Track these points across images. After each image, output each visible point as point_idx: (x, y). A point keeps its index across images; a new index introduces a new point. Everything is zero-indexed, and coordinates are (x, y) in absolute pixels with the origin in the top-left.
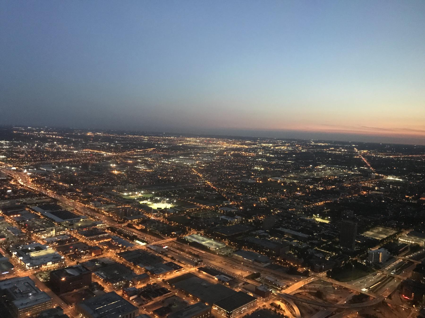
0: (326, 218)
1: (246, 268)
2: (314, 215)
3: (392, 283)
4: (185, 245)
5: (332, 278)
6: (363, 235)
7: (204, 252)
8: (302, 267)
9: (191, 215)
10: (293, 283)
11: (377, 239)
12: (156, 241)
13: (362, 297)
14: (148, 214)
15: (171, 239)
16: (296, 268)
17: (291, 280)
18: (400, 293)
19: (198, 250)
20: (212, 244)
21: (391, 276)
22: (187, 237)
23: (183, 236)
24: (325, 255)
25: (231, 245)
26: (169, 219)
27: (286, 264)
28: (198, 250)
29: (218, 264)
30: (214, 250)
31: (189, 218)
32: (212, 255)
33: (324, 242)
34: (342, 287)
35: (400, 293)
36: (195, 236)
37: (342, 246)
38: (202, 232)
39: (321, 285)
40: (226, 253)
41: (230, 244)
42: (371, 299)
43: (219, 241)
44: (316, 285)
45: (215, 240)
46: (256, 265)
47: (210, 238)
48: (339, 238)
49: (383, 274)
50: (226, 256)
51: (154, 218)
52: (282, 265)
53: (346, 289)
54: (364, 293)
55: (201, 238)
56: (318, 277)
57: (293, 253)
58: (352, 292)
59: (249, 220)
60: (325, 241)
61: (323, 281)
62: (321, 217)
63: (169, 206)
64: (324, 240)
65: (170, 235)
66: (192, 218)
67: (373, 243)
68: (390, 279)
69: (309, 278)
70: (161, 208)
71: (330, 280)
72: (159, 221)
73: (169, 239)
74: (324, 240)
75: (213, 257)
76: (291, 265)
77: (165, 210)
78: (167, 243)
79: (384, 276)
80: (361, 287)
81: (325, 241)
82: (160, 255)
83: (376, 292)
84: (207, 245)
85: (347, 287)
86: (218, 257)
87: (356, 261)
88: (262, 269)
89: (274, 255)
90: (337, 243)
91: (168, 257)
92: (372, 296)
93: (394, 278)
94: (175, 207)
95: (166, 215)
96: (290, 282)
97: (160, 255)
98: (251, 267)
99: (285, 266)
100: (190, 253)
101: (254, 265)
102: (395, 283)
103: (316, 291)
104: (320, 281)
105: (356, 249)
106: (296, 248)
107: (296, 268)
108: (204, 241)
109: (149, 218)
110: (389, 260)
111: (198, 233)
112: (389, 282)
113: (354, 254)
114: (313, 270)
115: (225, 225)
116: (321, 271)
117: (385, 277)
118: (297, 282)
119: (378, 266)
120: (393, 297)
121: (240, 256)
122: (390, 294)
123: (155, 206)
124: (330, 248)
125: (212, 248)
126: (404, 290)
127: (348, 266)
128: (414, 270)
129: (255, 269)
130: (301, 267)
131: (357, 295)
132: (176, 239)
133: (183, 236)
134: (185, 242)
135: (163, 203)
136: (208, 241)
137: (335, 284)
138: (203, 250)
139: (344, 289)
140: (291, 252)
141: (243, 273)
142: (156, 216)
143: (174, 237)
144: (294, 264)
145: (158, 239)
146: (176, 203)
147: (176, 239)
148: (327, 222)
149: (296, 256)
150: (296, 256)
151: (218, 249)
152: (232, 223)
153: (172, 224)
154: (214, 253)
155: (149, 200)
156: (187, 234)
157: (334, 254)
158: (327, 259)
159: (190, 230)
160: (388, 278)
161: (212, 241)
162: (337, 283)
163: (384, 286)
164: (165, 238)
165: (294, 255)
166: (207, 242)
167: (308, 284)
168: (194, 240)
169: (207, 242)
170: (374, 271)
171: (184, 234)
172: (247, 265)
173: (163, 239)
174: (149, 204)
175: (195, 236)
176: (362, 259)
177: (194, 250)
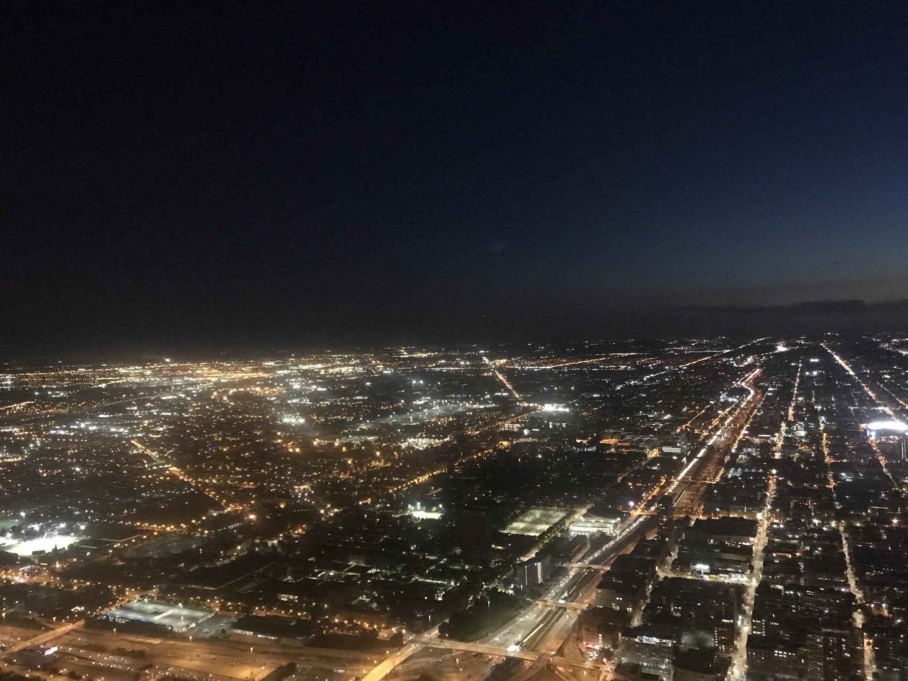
0: (434, 509)
1: (262, 658)
2: (410, 506)
3: (562, 622)
4: (107, 634)
5: (451, 637)
6: (505, 532)
7: (157, 641)
10: (370, 668)
11: (532, 534)
12: (25, 639)
13: (512, 663)
14: (7, 570)
15: (70, 627)
16: (374, 633)
17: (366, 663)
18: (579, 639)
19: (143, 640)
20: (177, 617)
21: (560, 608)
22: (115, 612)
23: (103, 612)
25: (227, 610)
26: (66, 575)
27: (355, 627)
28: (143, 640)
30: (184, 630)
32: (180, 643)
34: (471, 652)
35: (578, 640)
36: (139, 606)
37: (468, 564)
38: (154, 592)
40: (213, 632)
41: (223, 607)
42: (527, 664)
43: (196, 606)
45: (186, 605)
46: (283, 646)
47: (174, 604)
49: (546, 606)
50: (212, 640)
51: (22, 581)
52: (345, 632)
53: (479, 655)
54: (512, 655)
55: (151, 607)
56: (422, 643)
57: (368, 600)
58: (490, 660)
59: (270, 543)
60: (435, 558)
64: (431, 558)
65: (64, 614)
67: (523, 543)
68: (561, 611)
69: (403, 649)
70: (43, 552)
71: (447, 644)
72: (36, 587)
73: (62, 626)
74: (431, 558)
75: (184, 649)
76: (365, 629)
77: (57, 554)
79: (549, 609)
80: (504, 644)
81: (435, 558)
82: (37, 674)
83: (536, 646)
84: (167, 622)
85: (480, 651)
86: (196, 644)
87: (496, 589)
88: (299, 651)
89: (326, 612)
90: (454, 559)
91: (61, 674)
92: (529, 658)
93: (565, 609)
94: (82, 542)
95: (58, 566)
96: (361, 667)
97: (37, 674)
98: (274, 653)
99: (351, 633)
100: (120, 652)
101: (283, 646)
102: (569, 619)
103: (418, 677)
104: (427, 651)
105: (496, 562)
106: (376, 585)
107: (374, 633)
108: (157, 613)
109: (9, 581)
110: (555, 574)
111: (143, 597)
112: (558, 620)
113: (491, 575)
114: (412, 629)
115: (213, 563)
116: (427, 627)
117: (550, 612)
118: (378, 664)
119: (537, 592)
120: (566, 651)
121: (248, 633)
122: (559, 646)
123: (24, 548)
124: (445, 573)
125: (180, 626)
126: (584, 632)
128: (599, 587)
129: (284, 655)
130: (386, 628)
131: (500, 662)
132: (82, 623)
133: (103, 612)
134: (108, 624)
135: (50, 536)
136: (171, 611)
138: (154, 636)
139: (475, 656)
141: (256, 670)
142: (30, 573)
143: (78, 619)
144: (371, 625)
145: (30, 632)
146: (85, 532)
147: (82, 623)
148: (436, 516)
150: (375, 605)
151: (194, 625)
153: (72, 587)
154: (182, 637)
155: (9, 535)
156: (114, 604)
157: (453, 583)
158: (440, 599)
159: (121, 592)
160: (556, 613)
161: (180, 610)
162: (462, 646)
163: (549, 630)
164: (51, 626)
165: (371, 602)
166: (160, 616)
167: (401, 663)
168: (132, 616)
169: (164, 615)
170: (529, 604)
172: (263, 651)
173: (48, 629)
174: (10, 547)
175: (135, 604)
176: (507, 584)
177: (131, 641)
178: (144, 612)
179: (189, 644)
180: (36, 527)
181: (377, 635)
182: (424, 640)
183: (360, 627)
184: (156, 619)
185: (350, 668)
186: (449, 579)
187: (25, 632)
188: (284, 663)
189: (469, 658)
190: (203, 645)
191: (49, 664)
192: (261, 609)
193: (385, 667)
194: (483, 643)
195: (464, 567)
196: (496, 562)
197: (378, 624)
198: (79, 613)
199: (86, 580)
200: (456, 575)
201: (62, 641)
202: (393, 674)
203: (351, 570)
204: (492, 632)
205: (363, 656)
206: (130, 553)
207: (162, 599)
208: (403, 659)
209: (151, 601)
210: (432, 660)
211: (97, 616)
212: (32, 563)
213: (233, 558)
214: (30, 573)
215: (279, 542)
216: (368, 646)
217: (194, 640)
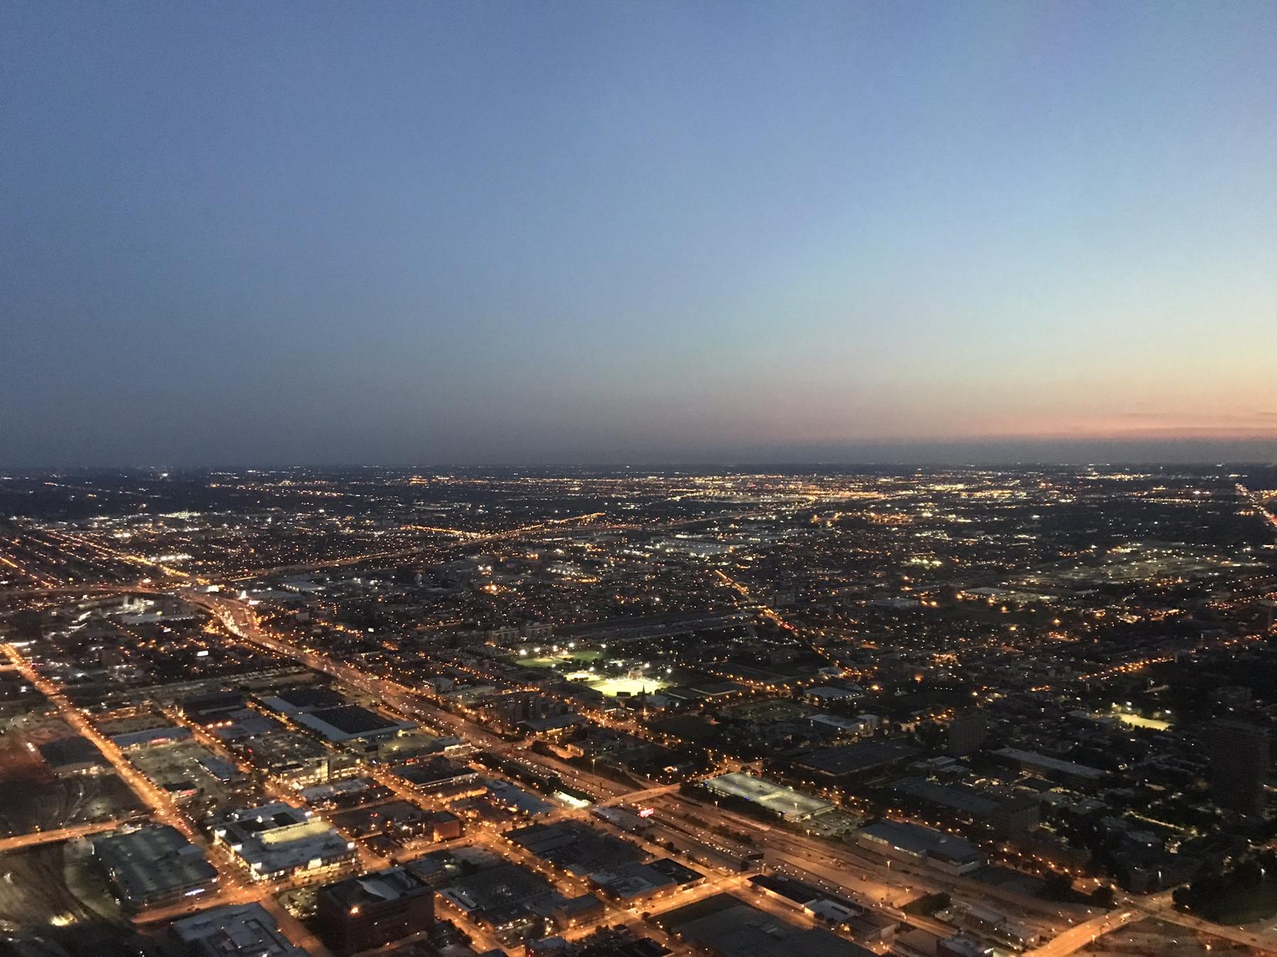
0: (1157, 715)
1: (900, 877)
2: (1114, 705)
4: (706, 807)
5: (1192, 912)
7: (766, 828)
8: (1089, 875)
9: (722, 714)
10: (1061, 928)
12: (618, 794)
14: (592, 710)
15: (664, 789)
16: (1066, 881)
17: (1054, 919)
22: (712, 781)
24: (1165, 835)
25: (851, 804)
26: (654, 726)
27: (1035, 865)
29: (811, 866)
31: (713, 722)
32: (793, 836)
33: (1159, 795)
34: (1230, 941)
36: (735, 779)
37: (1221, 808)
38: (757, 765)
39: (1156, 936)
40: (834, 831)
41: (845, 801)
43: (812, 792)
44: (1139, 935)
45: (798, 788)
47: (784, 785)
48: (1207, 780)
50: (834, 841)
52: (1019, 869)
53: (1243, 948)
55: (754, 784)
56: (1147, 911)
59: (904, 727)
60: (1161, 788)
61: (1164, 922)
62: (1140, 712)
63: (652, 686)
64: (1155, 787)
66: (724, 721)
69: (1114, 913)
70: (628, 694)
71: (1187, 921)
72: (623, 733)
74: (1155, 787)
76: (1050, 870)
78: (652, 800)
81: (1161, 788)
82: (631, 838)
84: (775, 806)
86: (811, 842)
88: (950, 880)
89: (989, 834)
90: (1201, 797)
91: (658, 844)
94: (670, 689)
95: (645, 713)
96: (1048, 925)
97: (631, 838)
98: (917, 875)
99: (1029, 872)
100: (722, 831)
101: (928, 868)
104: (1151, 922)
106: (1063, 812)
107: (1066, 881)
108: (763, 793)
109: (595, 723)
111: (744, 769)
114: (1126, 885)
115: (828, 742)
116: (1154, 888)
118: (1077, 923)
121: (881, 841)
123: (610, 687)
124: (1182, 814)
125: (792, 815)
127: (1245, 875)
129: (930, 880)
132: (677, 787)
134: (706, 796)
135: (634, 677)
136: (778, 794)
137: (1205, 933)
139: (1235, 947)
140: (1047, 826)
143: (673, 782)
144: (1060, 866)
147: (677, 787)
148: (1162, 726)
149: (1064, 840)
151: (809, 817)
152: (850, 737)
153: (663, 742)
154: (797, 829)
155: (592, 669)
156: (711, 771)
157: (1194, 832)
158: (1172, 851)
159: (718, 758)
161: (788, 793)
166: (773, 796)
168: (733, 790)
169: (773, 796)
171: (702, 771)
172: (905, 869)
173: (639, 788)
174: (593, 683)
177: (734, 821)
178: (747, 789)
179: (804, 839)
180: (620, 664)
181: (1071, 883)
182: (1147, 906)
183: (1043, 867)
184: (763, 799)
185: (1029, 920)
186: (1189, 825)
187: (615, 785)
188: (933, 892)
189: (1227, 949)
190: (824, 846)
191: (644, 829)
192: (896, 814)
193: (1088, 932)
194: (1251, 931)
195: (1213, 810)
196: (1271, 813)
197: (1072, 868)
198: (672, 773)
199: (678, 737)
200: (1203, 822)
201: (655, 804)
202: (1096, 946)
203: (1024, 783)
204: (1266, 918)
205: (1050, 908)
206: (725, 711)
207: (767, 776)
208: (1115, 927)
209: (755, 775)
210: (1162, 939)
211: (693, 782)
212: (617, 705)
213: (855, 739)
214: (616, 718)
215: (916, 726)
216: (1059, 899)
217: (812, 836)
